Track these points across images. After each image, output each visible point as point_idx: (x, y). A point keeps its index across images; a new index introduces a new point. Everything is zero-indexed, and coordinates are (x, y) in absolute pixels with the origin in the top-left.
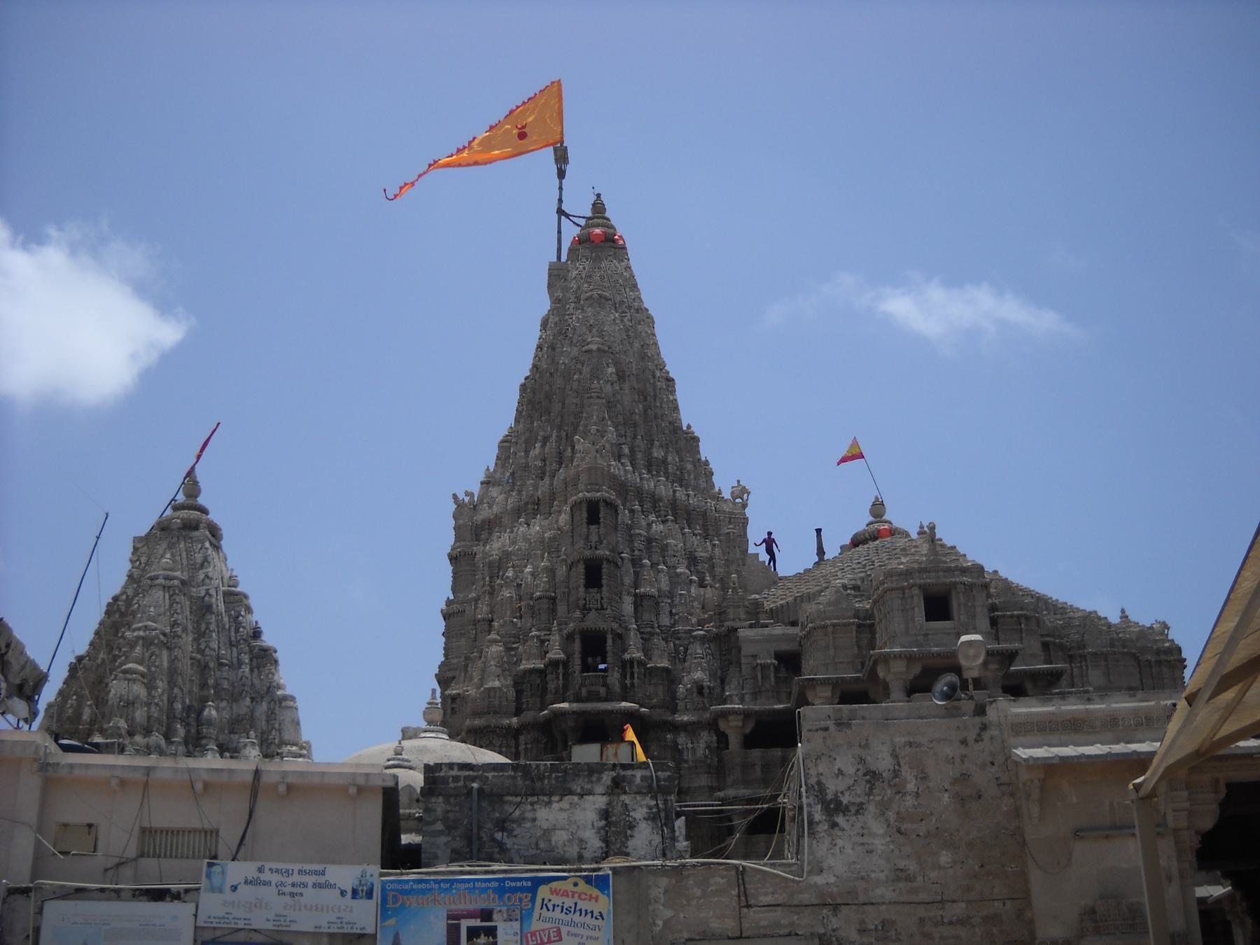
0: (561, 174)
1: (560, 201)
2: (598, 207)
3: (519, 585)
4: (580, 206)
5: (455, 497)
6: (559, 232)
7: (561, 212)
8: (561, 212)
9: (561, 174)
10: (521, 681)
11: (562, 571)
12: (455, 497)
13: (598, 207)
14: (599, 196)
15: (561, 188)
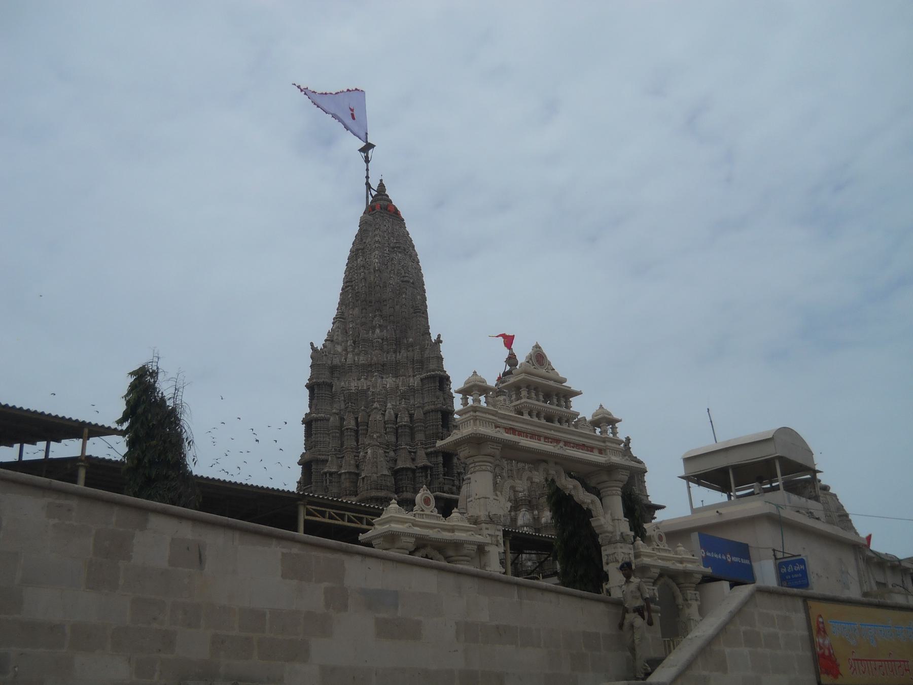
0: (367, 161)
1: (367, 177)
2: (382, 186)
3: (384, 415)
4: (375, 185)
5: (312, 344)
6: (367, 197)
7: (368, 184)
8: (368, 184)
9: (367, 161)
10: (396, 473)
11: (418, 414)
12: (312, 344)
13: (382, 186)
14: (381, 180)
15: (367, 170)
